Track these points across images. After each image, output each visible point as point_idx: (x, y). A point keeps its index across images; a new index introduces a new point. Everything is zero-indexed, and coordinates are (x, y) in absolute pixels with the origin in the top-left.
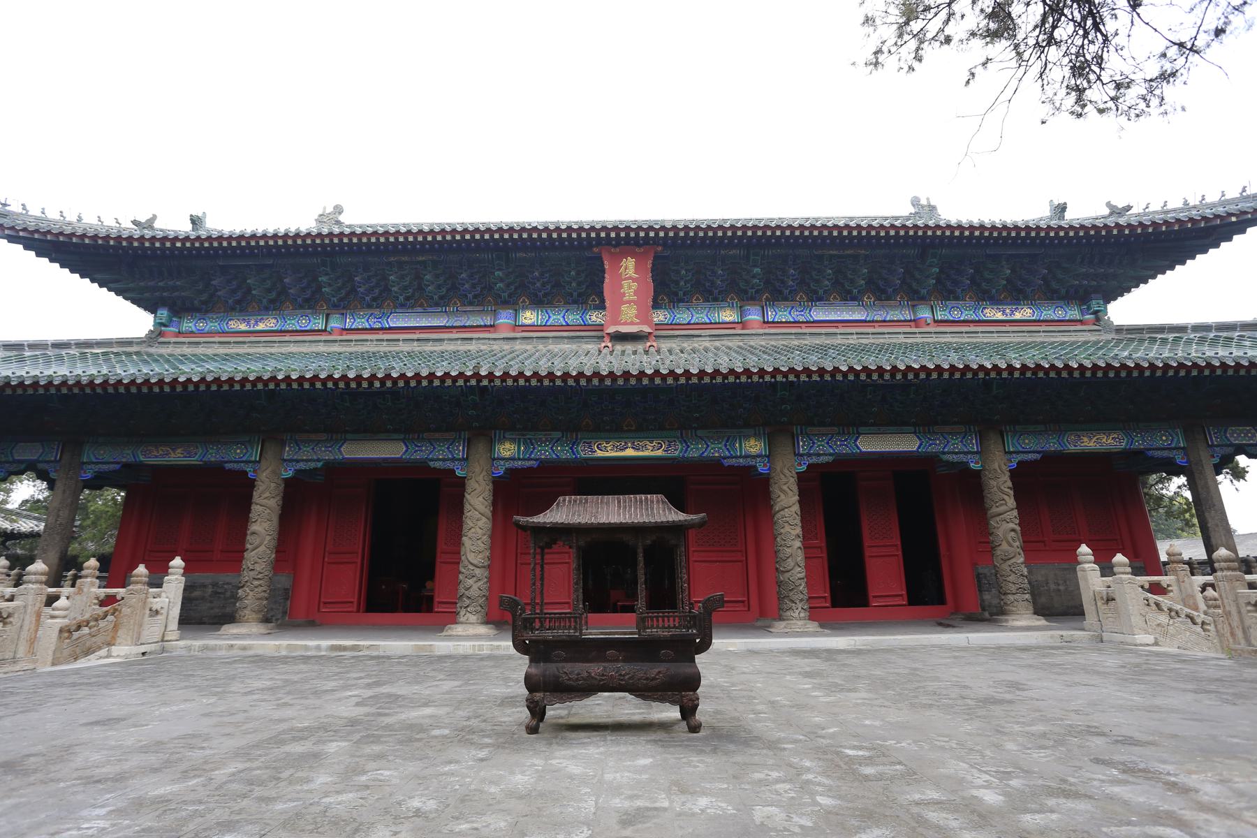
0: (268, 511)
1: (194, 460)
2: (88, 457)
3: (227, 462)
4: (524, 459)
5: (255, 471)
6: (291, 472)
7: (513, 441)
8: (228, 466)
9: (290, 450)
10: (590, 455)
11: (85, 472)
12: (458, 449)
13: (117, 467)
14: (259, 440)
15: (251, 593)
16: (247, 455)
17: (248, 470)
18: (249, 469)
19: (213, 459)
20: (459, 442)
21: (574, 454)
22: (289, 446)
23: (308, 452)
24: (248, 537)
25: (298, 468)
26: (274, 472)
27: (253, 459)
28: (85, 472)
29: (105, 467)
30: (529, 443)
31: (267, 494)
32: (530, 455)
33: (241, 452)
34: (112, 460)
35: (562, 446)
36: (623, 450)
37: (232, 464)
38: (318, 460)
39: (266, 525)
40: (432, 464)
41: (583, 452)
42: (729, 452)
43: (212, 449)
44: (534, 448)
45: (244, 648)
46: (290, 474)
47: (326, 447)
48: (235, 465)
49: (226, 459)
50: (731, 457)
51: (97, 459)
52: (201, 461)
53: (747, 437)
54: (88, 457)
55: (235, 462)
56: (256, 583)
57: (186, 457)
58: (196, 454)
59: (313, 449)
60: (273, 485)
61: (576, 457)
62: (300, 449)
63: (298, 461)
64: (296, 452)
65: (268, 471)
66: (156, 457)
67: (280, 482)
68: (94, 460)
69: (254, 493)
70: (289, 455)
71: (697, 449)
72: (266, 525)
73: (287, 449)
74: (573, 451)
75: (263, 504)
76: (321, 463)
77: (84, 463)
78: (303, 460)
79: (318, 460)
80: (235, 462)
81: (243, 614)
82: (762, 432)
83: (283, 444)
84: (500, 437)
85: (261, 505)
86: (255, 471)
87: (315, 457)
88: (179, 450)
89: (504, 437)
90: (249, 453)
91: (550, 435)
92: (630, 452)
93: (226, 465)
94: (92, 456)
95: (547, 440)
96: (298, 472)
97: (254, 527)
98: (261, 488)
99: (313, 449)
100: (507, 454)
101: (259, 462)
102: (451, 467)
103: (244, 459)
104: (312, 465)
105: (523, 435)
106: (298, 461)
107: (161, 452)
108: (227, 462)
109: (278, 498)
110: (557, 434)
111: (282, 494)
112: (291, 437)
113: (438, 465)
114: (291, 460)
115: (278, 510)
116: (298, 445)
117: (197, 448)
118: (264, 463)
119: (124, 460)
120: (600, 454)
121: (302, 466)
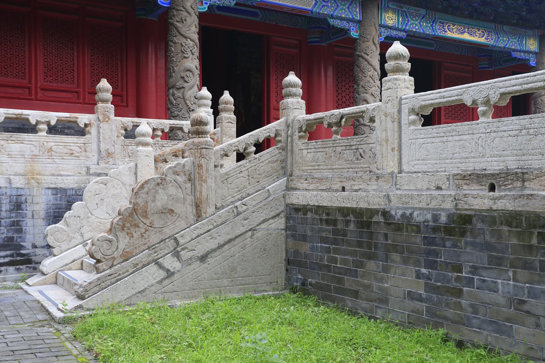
4: (400, 30)
7: (394, 11)
10: (442, 34)
12: (356, 11)
20: (356, 3)
21: (434, 31)
30: (405, 15)
32: (406, 26)
35: (426, 23)
36: (463, 33)
40: (331, 21)
41: (440, 33)
42: (520, 47)
44: (408, 21)
50: (520, 51)
53: (530, 37)
61: (435, 34)
71: (503, 40)
74: (433, 29)
82: (537, 34)
84: (385, 5)
89: (388, 6)
91: (419, 11)
92: (466, 37)
95: (416, 16)
100: (390, 23)
102: (347, 27)
105: (401, 7)
110: (423, 12)
113: (337, 23)
120: (449, 34)
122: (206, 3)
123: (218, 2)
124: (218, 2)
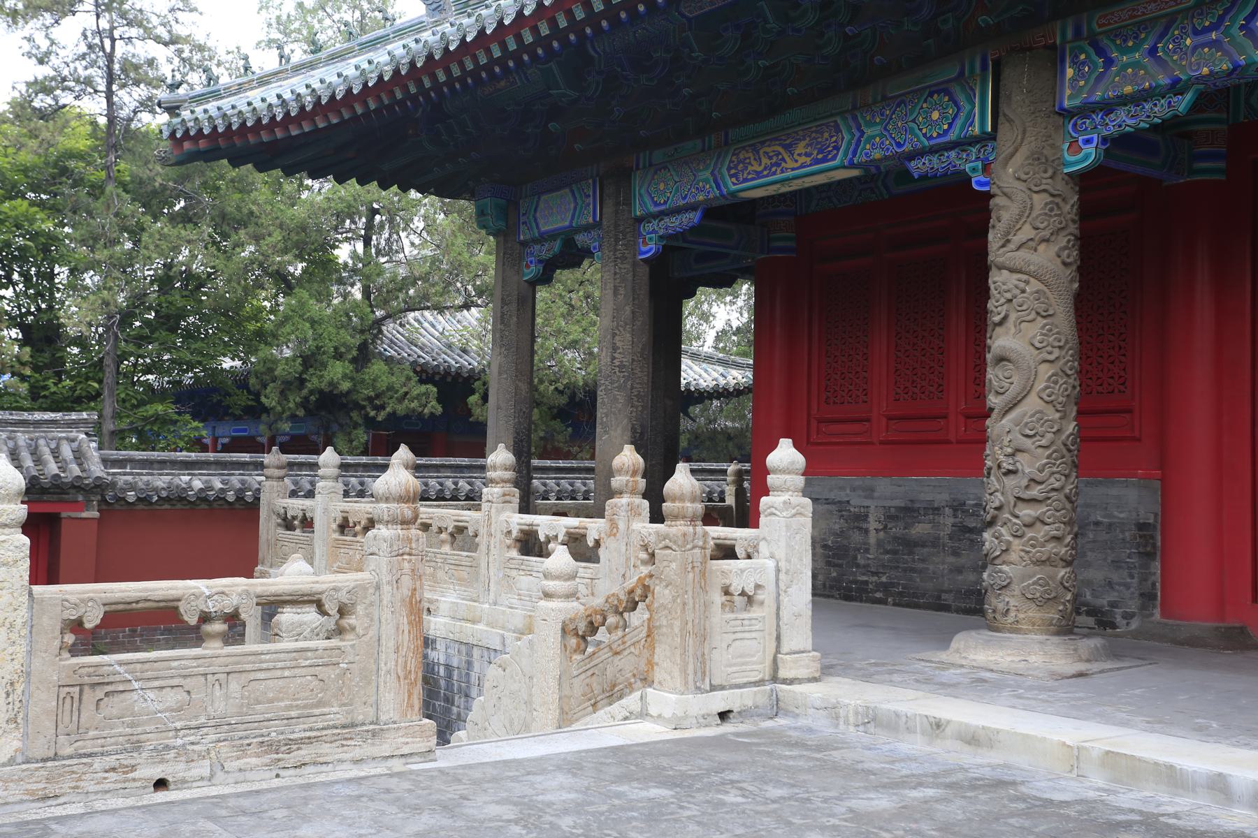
0: (1035, 285)
1: (836, 170)
2: (643, 204)
3: (912, 156)
5: (986, 168)
6: (1090, 150)
8: (918, 167)
9: (1079, 74)
11: (645, 243)
13: (694, 217)
14: (984, 68)
15: (1017, 544)
16: (959, 123)
17: (968, 167)
18: (969, 163)
19: (877, 154)
22: (1075, 63)
23: (1136, 65)
24: (992, 374)
25: (1111, 130)
26: (1036, 158)
27: (977, 130)
28: (645, 243)
29: (675, 223)
31: (1026, 232)
33: (943, 116)
34: (681, 203)
37: (926, 160)
38: (1176, 87)
39: (1034, 330)
43: (871, 124)
45: (973, 739)
46: (1087, 156)
47: (1196, 33)
48: (935, 159)
49: (907, 147)
51: (656, 204)
52: (852, 165)
54: (643, 204)
55: (933, 151)
56: (1027, 512)
57: (817, 162)
58: (837, 148)
59: (1153, 52)
60: (1040, 200)
62: (1109, 62)
63: (1107, 107)
64: (1100, 77)
65: (1019, 158)
66: (759, 175)
67: (1060, 186)
68: (653, 209)
69: (990, 236)
70: (1077, 91)
72: (1034, 330)
73: (1070, 72)
75: (1018, 264)
76: (1189, 97)
77: (640, 220)
78: (1123, 101)
79: (1176, 87)
80: (933, 151)
81: (1001, 606)
83: (1055, 58)
85: (1012, 271)
86: (986, 168)
87: (1163, 80)
88: (800, 148)
90: (962, 115)
93: (913, 163)
94: (646, 199)
96: (1118, 144)
97: (1001, 341)
98: (1005, 216)
99: (1153, 52)
101: (992, 137)
103: (953, 136)
104: (1158, 110)
106: (1107, 107)
107: (765, 161)
108: (912, 156)
109: (1063, 241)
111: (1073, 228)
112: (1078, 34)
114: (1086, 111)
115: (1066, 281)
116: (1100, 52)
117: (838, 130)
118: (1007, 136)
119: (701, 197)
121: (1124, 120)
122: (1088, 141)
123: (1129, 122)
124: (1129, 122)
